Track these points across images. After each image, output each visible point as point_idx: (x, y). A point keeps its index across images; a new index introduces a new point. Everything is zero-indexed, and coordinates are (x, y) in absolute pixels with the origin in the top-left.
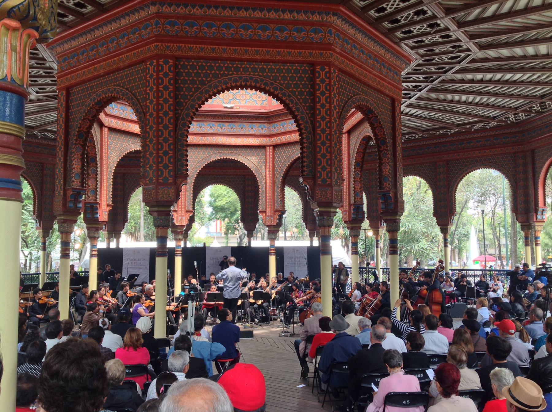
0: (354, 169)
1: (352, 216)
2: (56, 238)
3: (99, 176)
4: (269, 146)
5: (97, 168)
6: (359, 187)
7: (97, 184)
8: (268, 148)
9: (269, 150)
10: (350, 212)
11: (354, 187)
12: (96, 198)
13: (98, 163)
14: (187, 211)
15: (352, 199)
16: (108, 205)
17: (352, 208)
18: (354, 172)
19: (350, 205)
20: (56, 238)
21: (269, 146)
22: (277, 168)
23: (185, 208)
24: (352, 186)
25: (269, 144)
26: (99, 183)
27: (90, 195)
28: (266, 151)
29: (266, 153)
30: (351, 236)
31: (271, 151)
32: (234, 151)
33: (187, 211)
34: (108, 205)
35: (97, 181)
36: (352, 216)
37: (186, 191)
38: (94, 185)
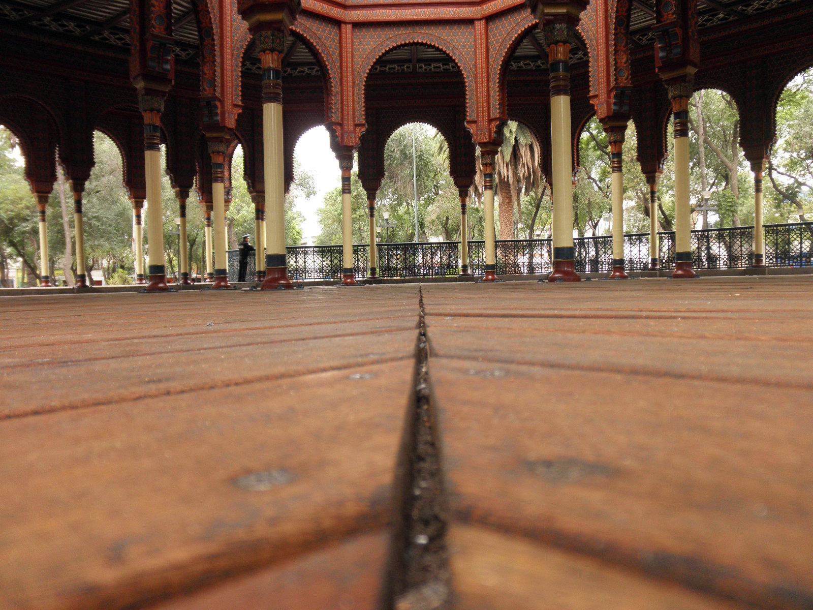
0: (615, 29)
1: (613, 107)
2: (194, 197)
3: (218, 59)
4: (480, 19)
5: (214, 45)
6: (624, 61)
7: (215, 71)
8: (477, 23)
9: (480, 26)
10: (609, 105)
11: (615, 59)
12: (215, 90)
13: (216, 37)
14: (356, 125)
15: (612, 79)
16: (235, 106)
17: (612, 95)
18: (615, 34)
19: (609, 92)
20: (194, 197)
21: (480, 19)
22: (492, 52)
23: (354, 121)
24: (612, 59)
25: (480, 16)
26: (218, 70)
27: (206, 88)
28: (474, 29)
29: (475, 31)
30: (610, 143)
31: (483, 26)
32: (425, 30)
33: (356, 125)
34: (235, 106)
35: (215, 66)
36: (613, 107)
37: (353, 95)
38: (211, 72)
